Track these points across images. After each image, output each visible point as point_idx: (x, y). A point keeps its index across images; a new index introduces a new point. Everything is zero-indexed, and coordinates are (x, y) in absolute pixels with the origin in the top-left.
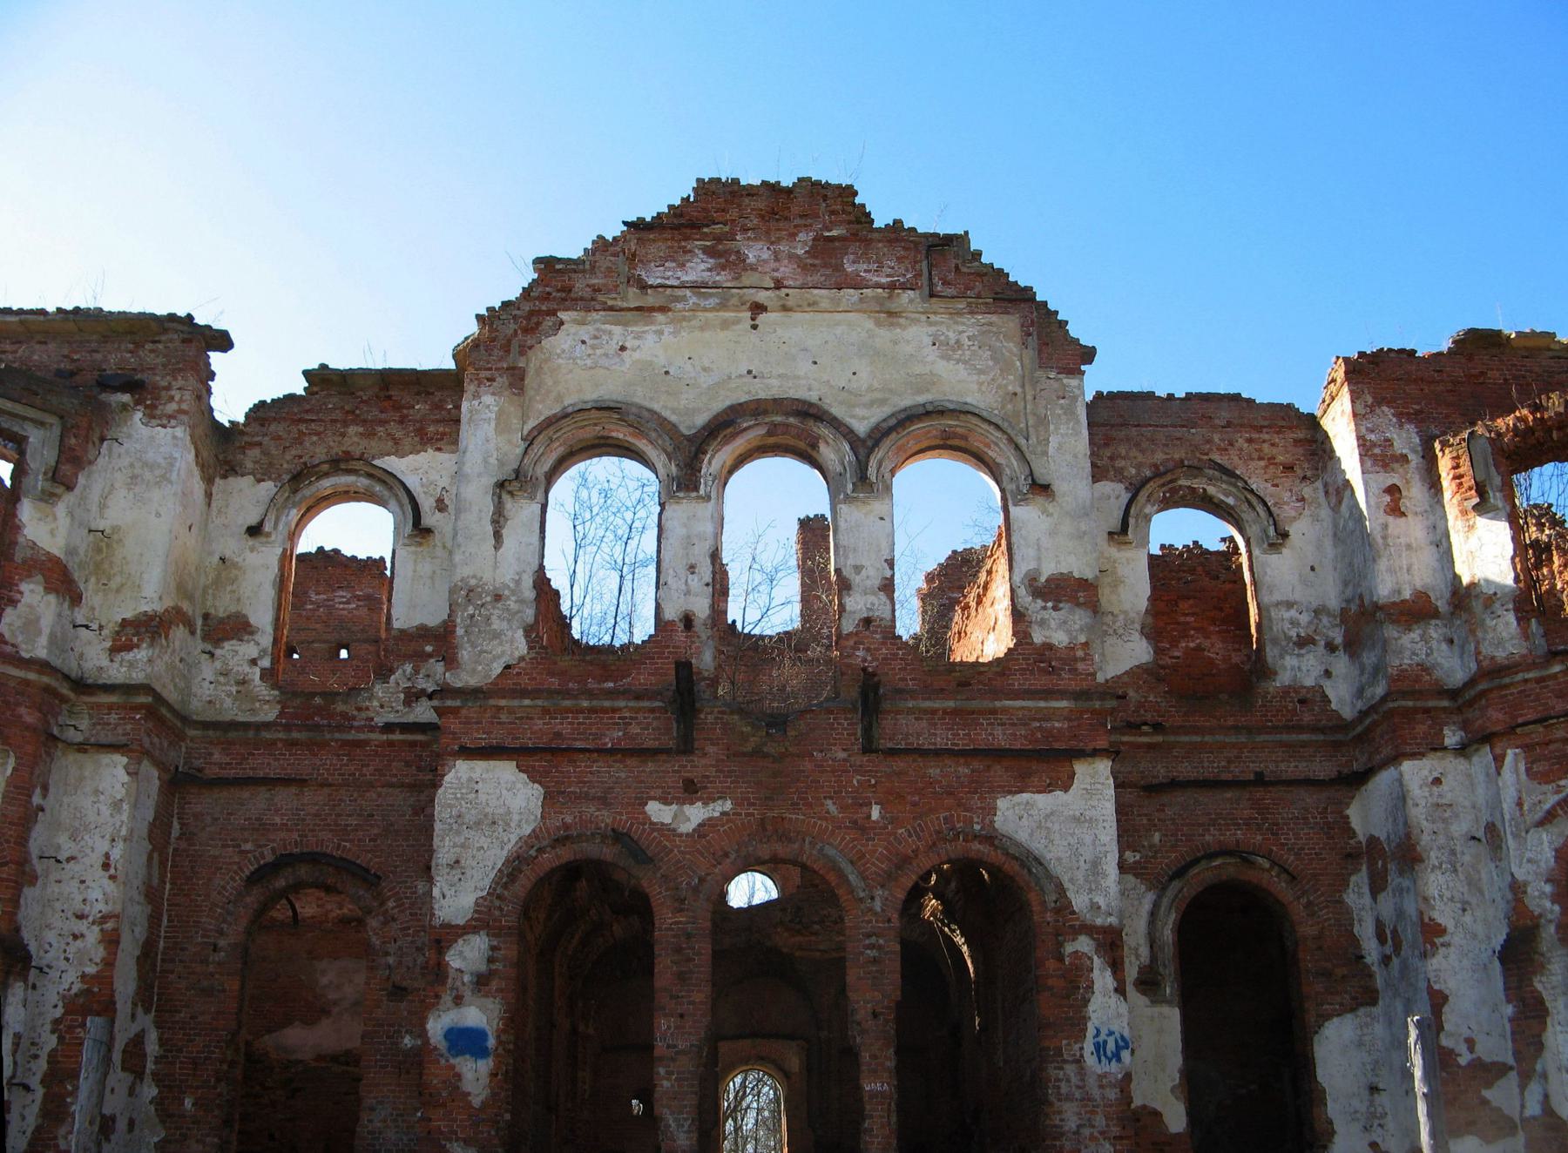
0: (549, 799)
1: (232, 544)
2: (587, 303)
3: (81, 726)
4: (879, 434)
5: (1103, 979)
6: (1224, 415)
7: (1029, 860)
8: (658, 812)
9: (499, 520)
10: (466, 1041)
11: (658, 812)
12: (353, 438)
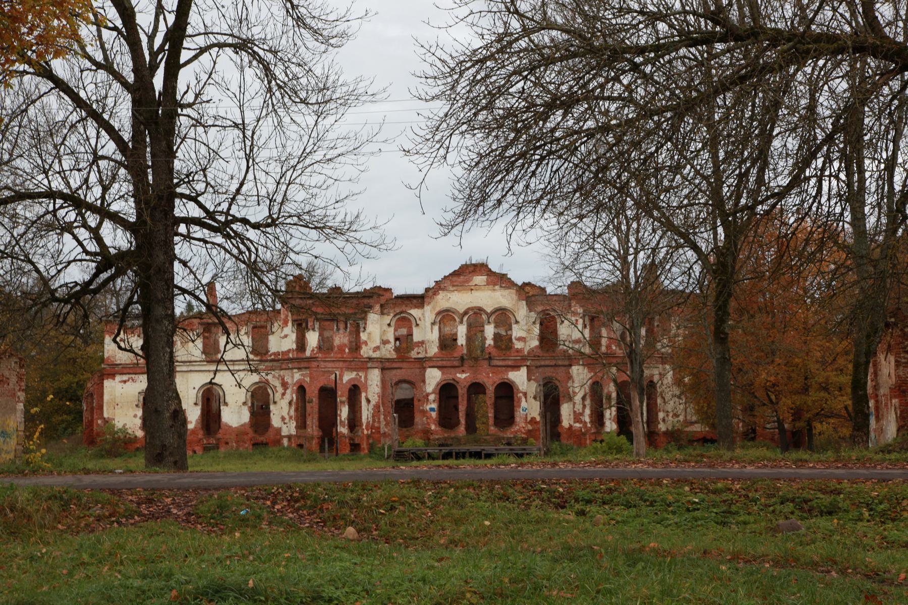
0: (443, 374)
1: (385, 327)
2: (443, 290)
3: (369, 365)
5: (523, 399)
6: (555, 298)
7: (513, 382)
8: (459, 375)
9: (432, 329)
10: (432, 409)
11: (459, 375)
12: (404, 308)
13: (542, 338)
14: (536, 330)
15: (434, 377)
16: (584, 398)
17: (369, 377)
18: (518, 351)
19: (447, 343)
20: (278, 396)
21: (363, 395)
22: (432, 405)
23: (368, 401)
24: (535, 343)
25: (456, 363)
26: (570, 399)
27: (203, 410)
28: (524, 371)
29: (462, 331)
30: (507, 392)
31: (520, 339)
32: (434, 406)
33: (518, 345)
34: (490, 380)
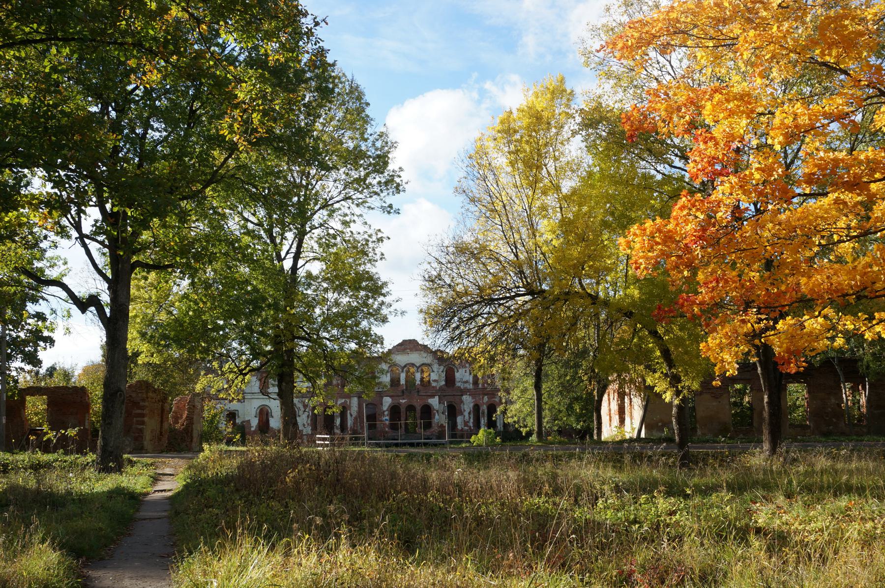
4: (420, 366)
10: (386, 420)
13: (446, 381)
14: (444, 375)
15: (387, 401)
16: (469, 413)
17: (352, 402)
18: (434, 387)
19: (395, 382)
20: (301, 412)
21: (348, 412)
22: (386, 418)
23: (351, 415)
24: (444, 383)
25: (400, 394)
26: (462, 414)
27: (259, 420)
28: (437, 398)
29: (403, 376)
30: (427, 411)
31: (435, 381)
32: (387, 418)
33: (434, 384)
34: (418, 404)
